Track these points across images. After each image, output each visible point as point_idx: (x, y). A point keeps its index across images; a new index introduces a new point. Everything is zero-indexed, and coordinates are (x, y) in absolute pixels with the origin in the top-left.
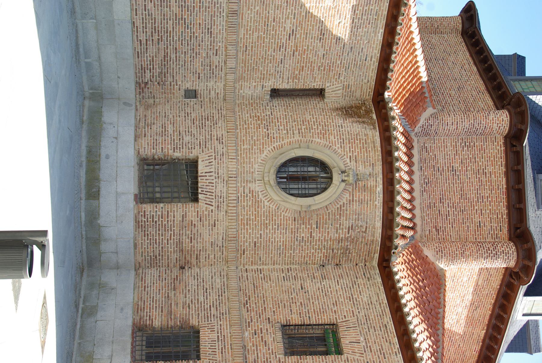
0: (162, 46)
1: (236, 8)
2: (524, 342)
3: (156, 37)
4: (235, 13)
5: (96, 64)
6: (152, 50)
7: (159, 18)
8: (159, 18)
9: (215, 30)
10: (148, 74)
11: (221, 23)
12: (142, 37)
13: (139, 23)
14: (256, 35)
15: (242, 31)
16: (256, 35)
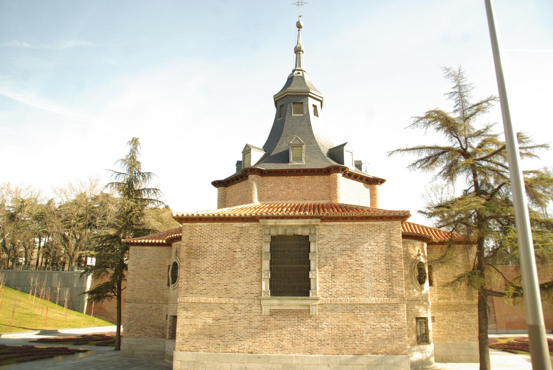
0: (147, 327)
1: (133, 301)
2: (359, 165)
3: (144, 329)
4: (135, 300)
5: (153, 352)
6: (148, 331)
7: (136, 328)
8: (136, 328)
9: (142, 308)
10: (159, 333)
11: (139, 305)
12: (143, 334)
13: (138, 335)
14: (145, 293)
15: (144, 298)
16: (145, 293)
